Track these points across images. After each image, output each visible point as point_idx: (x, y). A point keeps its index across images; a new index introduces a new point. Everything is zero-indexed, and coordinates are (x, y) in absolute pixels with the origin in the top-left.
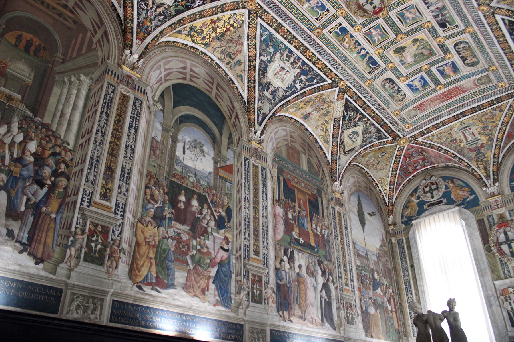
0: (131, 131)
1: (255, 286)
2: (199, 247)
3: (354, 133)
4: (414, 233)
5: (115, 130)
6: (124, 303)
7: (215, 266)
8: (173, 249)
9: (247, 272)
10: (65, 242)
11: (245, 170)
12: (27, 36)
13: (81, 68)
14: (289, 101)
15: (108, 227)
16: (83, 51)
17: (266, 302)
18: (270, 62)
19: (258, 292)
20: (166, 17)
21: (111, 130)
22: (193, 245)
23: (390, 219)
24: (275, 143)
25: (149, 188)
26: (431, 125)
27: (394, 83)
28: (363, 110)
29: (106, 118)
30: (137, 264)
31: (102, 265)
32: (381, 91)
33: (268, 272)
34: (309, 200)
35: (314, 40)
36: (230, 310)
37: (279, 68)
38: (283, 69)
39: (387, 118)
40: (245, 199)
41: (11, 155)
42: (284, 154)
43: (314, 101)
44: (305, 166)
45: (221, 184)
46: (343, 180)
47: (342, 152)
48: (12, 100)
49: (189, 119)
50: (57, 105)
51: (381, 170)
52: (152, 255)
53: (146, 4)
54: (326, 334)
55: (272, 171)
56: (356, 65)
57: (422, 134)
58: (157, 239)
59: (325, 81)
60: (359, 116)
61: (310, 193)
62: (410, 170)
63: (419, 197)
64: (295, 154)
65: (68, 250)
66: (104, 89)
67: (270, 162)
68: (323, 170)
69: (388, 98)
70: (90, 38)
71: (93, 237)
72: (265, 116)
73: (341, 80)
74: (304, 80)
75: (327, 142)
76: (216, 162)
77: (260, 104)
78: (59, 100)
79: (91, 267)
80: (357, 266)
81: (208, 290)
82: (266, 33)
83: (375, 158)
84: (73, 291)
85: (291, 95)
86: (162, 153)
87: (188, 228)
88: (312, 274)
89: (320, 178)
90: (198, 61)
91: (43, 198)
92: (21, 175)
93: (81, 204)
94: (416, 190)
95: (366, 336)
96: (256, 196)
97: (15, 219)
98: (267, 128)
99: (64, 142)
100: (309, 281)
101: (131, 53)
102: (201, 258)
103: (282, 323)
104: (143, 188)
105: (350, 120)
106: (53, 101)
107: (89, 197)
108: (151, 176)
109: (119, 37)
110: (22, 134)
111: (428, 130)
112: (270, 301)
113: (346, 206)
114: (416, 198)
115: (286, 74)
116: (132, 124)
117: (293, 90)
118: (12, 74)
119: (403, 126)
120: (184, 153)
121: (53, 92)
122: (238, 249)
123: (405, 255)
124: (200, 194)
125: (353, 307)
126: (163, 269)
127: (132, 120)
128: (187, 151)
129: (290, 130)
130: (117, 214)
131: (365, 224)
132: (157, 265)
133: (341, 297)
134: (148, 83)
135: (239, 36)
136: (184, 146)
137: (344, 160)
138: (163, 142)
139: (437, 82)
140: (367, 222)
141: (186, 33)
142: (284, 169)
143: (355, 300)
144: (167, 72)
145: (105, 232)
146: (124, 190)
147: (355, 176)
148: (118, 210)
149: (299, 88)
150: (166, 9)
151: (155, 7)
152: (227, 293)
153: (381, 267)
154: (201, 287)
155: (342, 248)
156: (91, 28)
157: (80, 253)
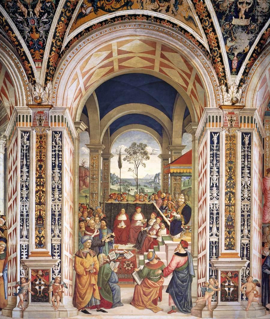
0: (55, 171)
1: (227, 284)
2: (147, 261)
5: (39, 177)
7: (169, 274)
8: (116, 271)
17: (244, 297)
19: (232, 289)
25: (83, 221)
29: (27, 170)
30: (80, 294)
31: (47, 301)
33: (249, 265)
40: (212, 187)
45: (173, 183)
52: (94, 281)
58: (98, 266)
76: (164, 158)
77: (229, 44)
79: (39, 305)
81: (160, 300)
86: (93, 179)
87: (133, 245)
93: (21, 258)
107: (26, 250)
108: (84, 208)
112: (251, 296)
116: (55, 163)
120: (120, 166)
124: (145, 204)
127: (54, 159)
128: (124, 163)
130: (55, 256)
136: (120, 158)
138: (93, 166)
145: (46, 274)
146: (57, 232)
148: (55, 252)
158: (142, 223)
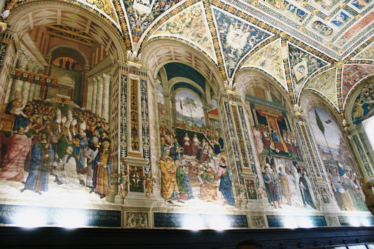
3: (301, 67)
4: (363, 129)
6: (162, 213)
8: (187, 173)
9: (242, 179)
10: (116, 181)
11: (226, 111)
12: (65, 59)
13: (102, 70)
14: (247, 56)
15: (141, 167)
16: (101, 59)
18: (227, 33)
19: (253, 191)
20: (149, 22)
21: (130, 105)
22: (200, 168)
23: (343, 123)
24: (244, 88)
25: (163, 136)
26: (358, 46)
27: (321, 23)
28: (303, 48)
30: (165, 187)
31: (142, 191)
32: (312, 31)
33: (257, 177)
34: (278, 121)
35: (254, 10)
36: (235, 207)
37: (234, 36)
38: (238, 35)
39: (323, 50)
41: (72, 134)
42: (253, 93)
43: (266, 52)
44: (270, 99)
46: (301, 102)
47: (295, 82)
48: (65, 100)
49: (180, 85)
50: (93, 97)
51: (328, 88)
52: (174, 180)
53: (134, 17)
54: (309, 213)
55: (246, 106)
56: (289, 18)
57: (353, 54)
58: (175, 169)
59: (270, 35)
60: (302, 54)
61: (277, 116)
62: (351, 83)
63: (362, 102)
64: (261, 92)
65: (119, 186)
66: (120, 79)
67: (243, 101)
68: (284, 98)
69: (319, 35)
70: (104, 49)
71: (133, 175)
72: (233, 70)
73: (281, 31)
74: (255, 39)
75: (283, 78)
76: (205, 110)
77: (227, 64)
78: (93, 94)
80: (324, 161)
81: (216, 196)
82: (219, 14)
83: (321, 81)
84: (128, 211)
85: (248, 52)
86: (167, 112)
87: (195, 157)
88: (290, 173)
89: (283, 104)
90: (177, 45)
91: (96, 157)
92: (80, 145)
93: (121, 156)
94: (359, 97)
95: (341, 210)
96: (238, 126)
97: (83, 174)
98: (236, 78)
99: (102, 119)
100: (289, 177)
101: (132, 51)
102: (207, 176)
103: (275, 210)
104: (159, 137)
105: (296, 58)
106: (89, 95)
109: (122, 43)
110: (76, 120)
111: (357, 51)
112: (263, 196)
113: (307, 120)
114: (360, 102)
115: (240, 38)
117: (248, 48)
118: (62, 85)
119: (337, 53)
120: (182, 108)
121: (89, 89)
122: (233, 165)
123: (360, 146)
124: (198, 133)
125: (326, 190)
126: (183, 187)
128: (183, 107)
129: (254, 76)
131: (324, 130)
132: (178, 186)
133: (316, 185)
134: (147, 68)
135: (201, 21)
137: (298, 88)
139: (355, 13)
140: (325, 129)
141: (165, 28)
142: (255, 104)
143: (327, 185)
144: (158, 58)
145: (140, 170)
146: (146, 141)
147: (310, 97)
149: (252, 45)
150: (148, 17)
151: (140, 18)
152: (231, 195)
153: (343, 158)
154: (212, 195)
155: (309, 150)
156: (103, 43)
157: (127, 187)
158: (198, 144)
